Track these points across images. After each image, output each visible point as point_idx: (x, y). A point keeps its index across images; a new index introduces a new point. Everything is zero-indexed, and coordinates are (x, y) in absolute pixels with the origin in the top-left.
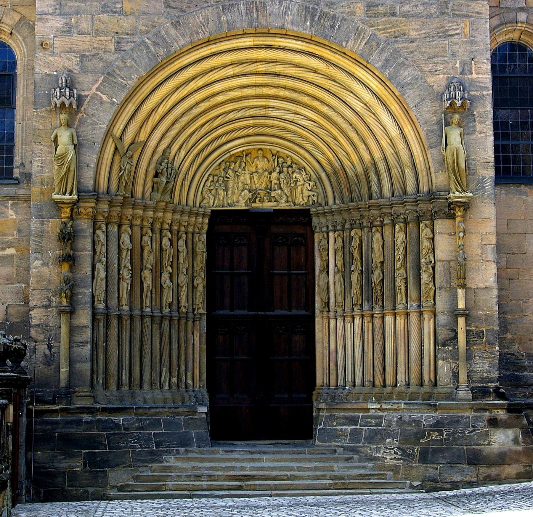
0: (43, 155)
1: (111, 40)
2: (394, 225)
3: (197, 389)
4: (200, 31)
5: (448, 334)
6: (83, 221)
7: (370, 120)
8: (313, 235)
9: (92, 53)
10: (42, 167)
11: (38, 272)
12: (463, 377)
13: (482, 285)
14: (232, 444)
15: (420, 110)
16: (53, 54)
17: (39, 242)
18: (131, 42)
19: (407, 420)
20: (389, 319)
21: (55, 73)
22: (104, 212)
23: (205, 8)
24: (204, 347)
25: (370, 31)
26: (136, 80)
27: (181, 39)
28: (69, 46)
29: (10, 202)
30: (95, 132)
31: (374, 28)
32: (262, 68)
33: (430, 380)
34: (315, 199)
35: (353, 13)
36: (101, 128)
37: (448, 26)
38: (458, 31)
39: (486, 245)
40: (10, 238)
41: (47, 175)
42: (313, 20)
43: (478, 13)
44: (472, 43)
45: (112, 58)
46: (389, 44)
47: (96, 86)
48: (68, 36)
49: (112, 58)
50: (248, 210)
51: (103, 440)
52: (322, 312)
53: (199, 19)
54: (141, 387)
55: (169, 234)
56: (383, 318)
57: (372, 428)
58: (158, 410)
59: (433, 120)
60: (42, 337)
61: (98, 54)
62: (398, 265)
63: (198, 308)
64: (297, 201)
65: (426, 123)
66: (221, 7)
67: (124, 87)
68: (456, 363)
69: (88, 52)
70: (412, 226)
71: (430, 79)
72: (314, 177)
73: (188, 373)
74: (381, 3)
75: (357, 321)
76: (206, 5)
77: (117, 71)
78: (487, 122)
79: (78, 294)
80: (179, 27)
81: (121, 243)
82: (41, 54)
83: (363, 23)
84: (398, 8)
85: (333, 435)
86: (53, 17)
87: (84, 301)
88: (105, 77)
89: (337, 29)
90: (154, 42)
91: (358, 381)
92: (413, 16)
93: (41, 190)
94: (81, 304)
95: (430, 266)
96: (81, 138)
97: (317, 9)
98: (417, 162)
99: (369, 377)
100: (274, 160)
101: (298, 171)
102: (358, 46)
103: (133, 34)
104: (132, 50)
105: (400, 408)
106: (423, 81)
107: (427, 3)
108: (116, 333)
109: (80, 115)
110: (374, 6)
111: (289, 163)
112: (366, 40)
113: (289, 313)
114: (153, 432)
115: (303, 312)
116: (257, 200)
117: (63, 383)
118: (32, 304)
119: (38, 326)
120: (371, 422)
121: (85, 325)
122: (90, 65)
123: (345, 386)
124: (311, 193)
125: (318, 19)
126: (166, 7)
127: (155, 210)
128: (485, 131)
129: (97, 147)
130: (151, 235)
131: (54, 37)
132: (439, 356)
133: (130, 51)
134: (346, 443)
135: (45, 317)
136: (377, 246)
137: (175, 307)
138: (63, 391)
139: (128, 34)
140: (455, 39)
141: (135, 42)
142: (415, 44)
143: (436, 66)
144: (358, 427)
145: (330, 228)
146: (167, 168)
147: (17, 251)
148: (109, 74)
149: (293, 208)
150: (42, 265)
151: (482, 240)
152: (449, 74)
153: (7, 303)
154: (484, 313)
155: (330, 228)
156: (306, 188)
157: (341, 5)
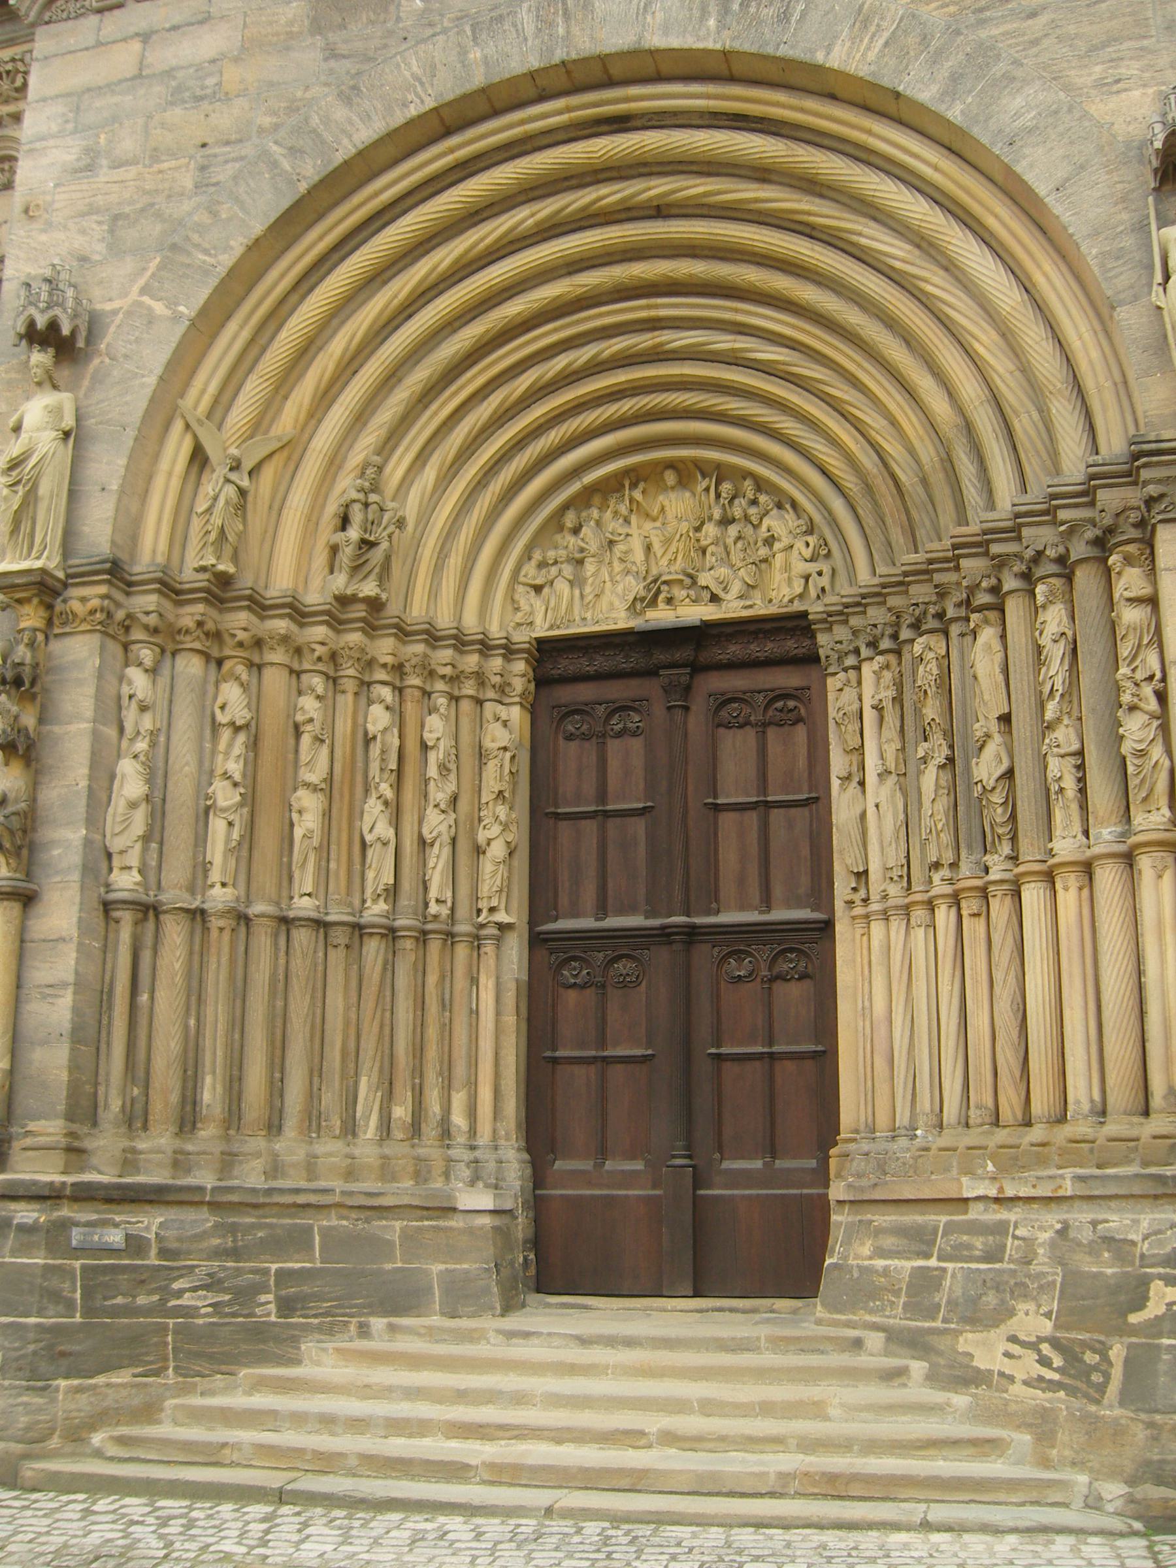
1: (189, 163)
4: (410, 97)
6: (80, 638)
7: (936, 283)
9: (138, 206)
14: (586, 1307)
16: (49, 226)
18: (235, 160)
19: (1086, 1235)
20: (1033, 895)
22: (147, 613)
23: (424, 41)
24: (510, 1020)
27: (361, 126)
28: (87, 200)
32: (610, 194)
34: (825, 581)
36: (143, 386)
45: (187, 206)
46: (958, 33)
47: (141, 282)
48: (87, 177)
52: (850, 903)
54: (274, 1126)
55: (386, 693)
57: (974, 1266)
58: (301, 1199)
61: (153, 205)
63: (492, 910)
65: (1095, 233)
67: (206, 272)
70: (1086, 578)
71: (1099, 108)
73: (453, 1093)
76: (429, 32)
77: (196, 237)
80: (356, 100)
81: (218, 711)
82: (22, 233)
89: (798, 22)
90: (291, 148)
94: (57, 873)
95: (1148, 690)
96: (93, 421)
98: (1083, 367)
99: (982, 1095)
100: (707, 489)
101: (775, 511)
103: (241, 141)
104: (235, 178)
105: (1061, 1193)
106: (1077, 114)
108: (177, 966)
109: (96, 362)
111: (750, 495)
112: (886, 35)
114: (274, 1267)
116: (661, 597)
120: (969, 1247)
121: (64, 934)
124: (812, 568)
126: (326, 59)
127: (336, 623)
131: (57, 186)
134: (896, 1318)
139: (228, 143)
141: (242, 158)
142: (1043, 19)
143: (1115, 68)
144: (933, 1262)
145: (865, 652)
146: (366, 505)
148: (174, 247)
149: (762, 612)
155: (865, 652)
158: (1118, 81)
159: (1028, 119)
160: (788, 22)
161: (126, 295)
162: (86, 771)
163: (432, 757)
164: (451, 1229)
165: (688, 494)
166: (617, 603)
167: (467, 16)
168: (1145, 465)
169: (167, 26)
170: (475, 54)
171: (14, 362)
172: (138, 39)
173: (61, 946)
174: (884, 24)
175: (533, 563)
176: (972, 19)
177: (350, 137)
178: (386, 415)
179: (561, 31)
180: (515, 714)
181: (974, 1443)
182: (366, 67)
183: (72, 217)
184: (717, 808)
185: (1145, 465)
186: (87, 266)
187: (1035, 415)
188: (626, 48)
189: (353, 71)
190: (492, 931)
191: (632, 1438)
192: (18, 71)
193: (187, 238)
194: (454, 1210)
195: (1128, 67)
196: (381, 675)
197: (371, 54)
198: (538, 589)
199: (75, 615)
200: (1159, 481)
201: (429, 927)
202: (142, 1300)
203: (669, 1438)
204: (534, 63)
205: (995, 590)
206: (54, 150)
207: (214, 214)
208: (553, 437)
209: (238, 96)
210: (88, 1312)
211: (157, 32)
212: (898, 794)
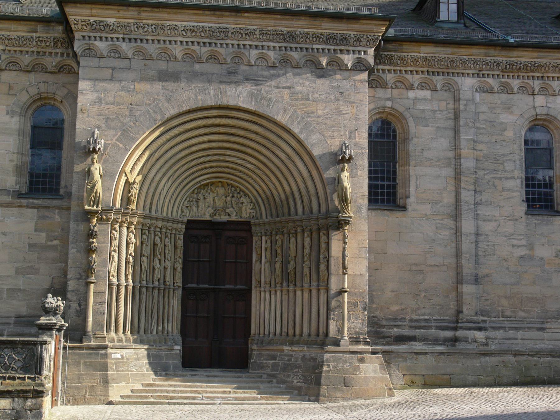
2: (304, 234)
3: (175, 334)
7: (291, 166)
8: (252, 238)
10: (79, 189)
11: (74, 256)
16: (88, 117)
18: (139, 110)
20: (299, 293)
21: (89, 129)
29: (57, 211)
30: (114, 167)
33: (323, 332)
34: (254, 214)
37: (342, 108)
38: (348, 112)
40: (56, 233)
42: (256, 101)
43: (361, 101)
47: (116, 138)
50: (210, 221)
55: (160, 234)
56: (295, 292)
60: (75, 298)
62: (306, 259)
64: (242, 216)
72: (254, 200)
75: (279, 293)
76: (188, 88)
77: (130, 129)
82: (81, 116)
85: (261, 366)
86: (90, 93)
89: (272, 107)
95: (325, 260)
98: (319, 193)
99: (285, 329)
102: (284, 119)
104: (140, 115)
111: (238, 191)
112: (289, 115)
113: (235, 287)
115: (244, 287)
116: (217, 214)
118: (69, 276)
119: (73, 291)
120: (285, 358)
123: (270, 335)
124: (252, 211)
128: (363, 175)
130: (148, 234)
135: (78, 286)
136: (292, 246)
137: (162, 281)
139: (137, 105)
141: (141, 111)
142: (321, 118)
144: (277, 361)
147: (60, 242)
148: (124, 130)
149: (240, 220)
150: (78, 251)
153: (53, 276)
155: (263, 233)
156: (248, 208)
159: (315, 141)
161: (112, 140)
163: (167, 248)
164: (173, 354)
165: (223, 188)
166: (207, 213)
170: (200, 98)
171: (81, 151)
172: (110, 69)
175: (187, 201)
177: (169, 111)
178: (164, 170)
180: (182, 237)
184: (226, 262)
187: (308, 197)
190: (177, 287)
192: (48, 41)
194: (173, 349)
196: (158, 230)
198: (187, 207)
199: (103, 219)
201: (166, 287)
205: (296, 231)
207: (135, 124)
208: (197, 174)
210: (117, 371)
211: (116, 68)
212: (270, 267)
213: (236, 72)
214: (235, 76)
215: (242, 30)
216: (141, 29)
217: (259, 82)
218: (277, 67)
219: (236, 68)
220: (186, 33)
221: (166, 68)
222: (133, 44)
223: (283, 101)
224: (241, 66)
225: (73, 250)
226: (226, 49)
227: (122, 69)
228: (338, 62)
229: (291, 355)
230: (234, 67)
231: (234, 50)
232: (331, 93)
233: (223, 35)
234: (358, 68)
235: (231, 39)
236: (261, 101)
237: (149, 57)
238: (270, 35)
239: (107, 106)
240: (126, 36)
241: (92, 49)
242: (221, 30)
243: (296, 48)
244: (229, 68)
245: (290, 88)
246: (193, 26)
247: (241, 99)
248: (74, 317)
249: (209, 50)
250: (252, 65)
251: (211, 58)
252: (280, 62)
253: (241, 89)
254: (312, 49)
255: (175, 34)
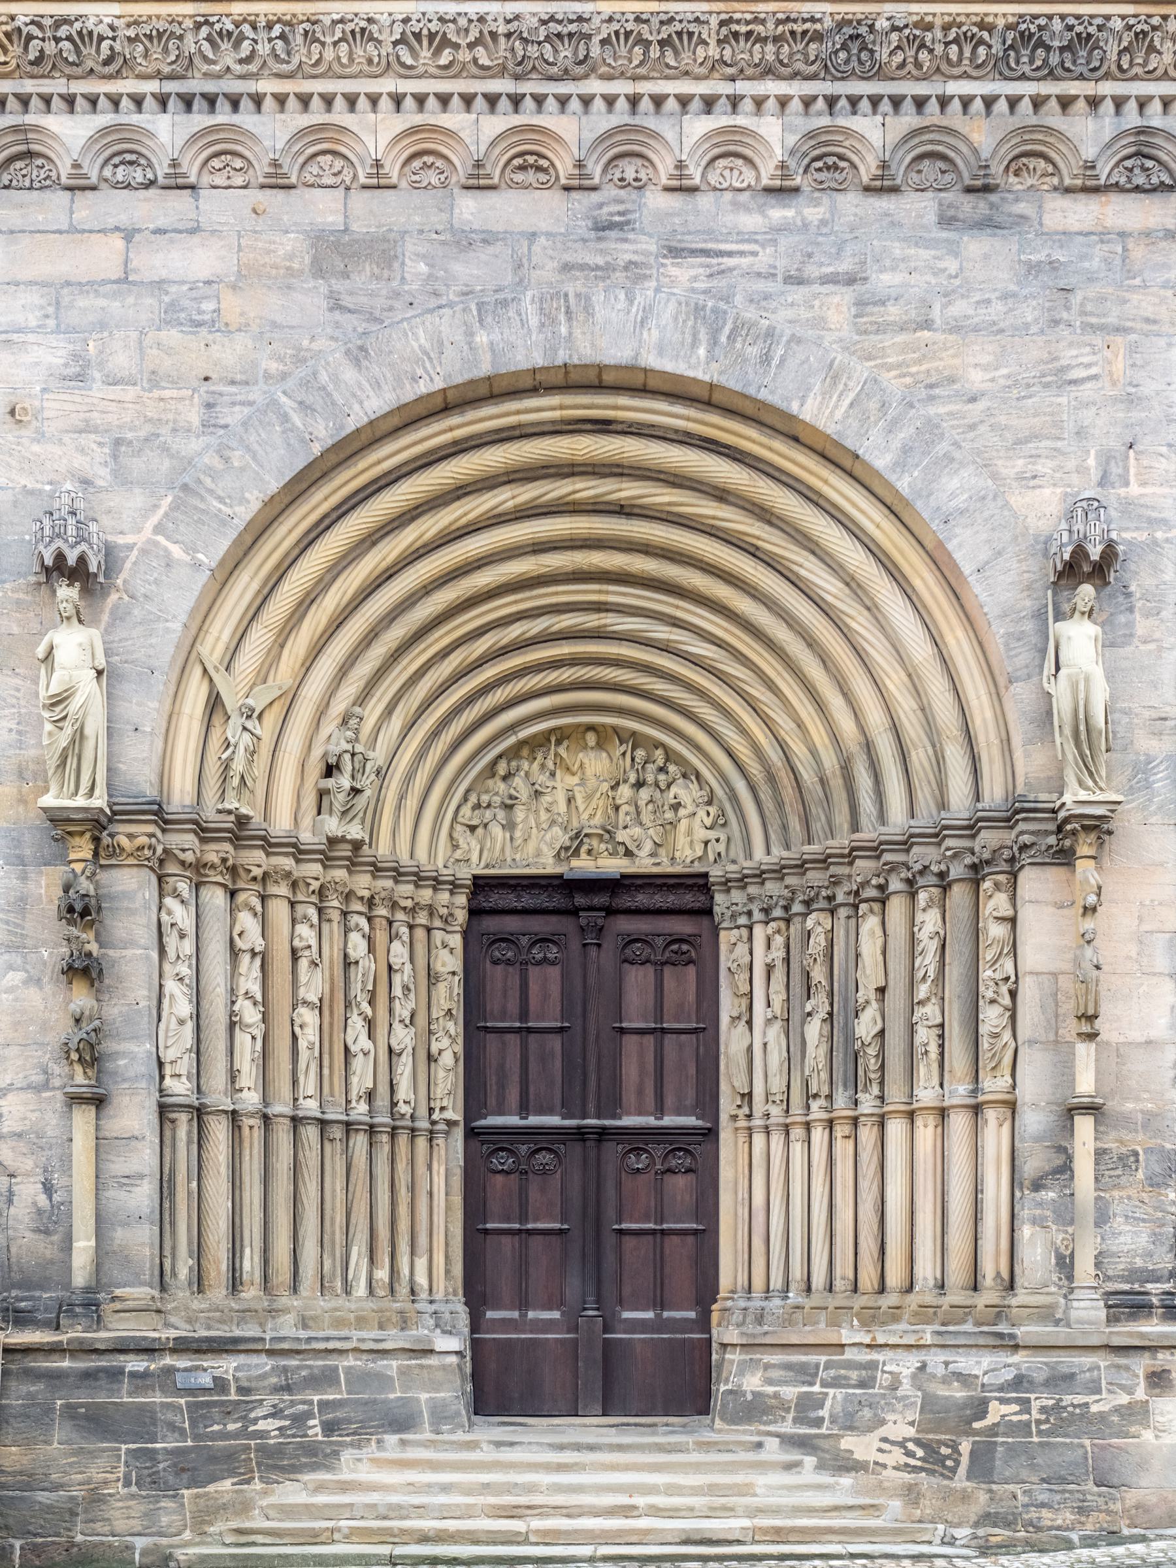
0: (23, 703)
4: (420, 372)
5: (1049, 1160)
6: (127, 870)
9: (142, 434)
10: (19, 733)
11: (16, 1000)
12: (1085, 1267)
13: (1137, 1036)
15: (990, 581)
16: (40, 437)
17: (17, 925)
18: (242, 403)
19: (940, 1371)
21: (48, 488)
23: (431, 311)
25: (862, 370)
26: (256, 506)
27: (371, 394)
28: (82, 415)
30: (153, 641)
31: (872, 363)
35: (820, 323)
36: (167, 630)
37: (1068, 355)
38: (1094, 371)
39: (1152, 932)
41: (32, 753)
42: (714, 342)
43: (1147, 320)
44: (1130, 401)
45: (194, 445)
46: (911, 406)
47: (154, 519)
49: (194, 445)
51: (178, 1418)
53: (417, 340)
59: (1024, 609)
60: (28, 1164)
61: (158, 435)
66: (473, 307)
67: (224, 521)
68: (1066, 1232)
69: (130, 430)
71: (1018, 499)
74: (894, 295)
76: (433, 302)
77: (208, 481)
78: (1164, 614)
79: (116, 1055)
80: (365, 363)
82: (10, 437)
83: (845, 349)
84: (937, 308)
86: (39, 338)
87: (131, 1074)
88: (176, 497)
89: (778, 366)
90: (301, 403)
91: (819, 1280)
92: (976, 329)
93: (20, 792)
94: (124, 1080)
97: (725, 312)
103: (247, 383)
104: (245, 424)
106: (1000, 503)
107: (1014, 295)
109: (113, 597)
110: (875, 304)
112: (851, 396)
117: (80, 1278)
119: (19, 1135)
121: (136, 1133)
122: (137, 465)
125: (729, 337)
126: (331, 310)
128: (1157, 635)
129: (161, 683)
131: (44, 390)
132: (1024, 1213)
133: (240, 429)
135: (37, 1114)
138: (77, 1299)
139: (233, 383)
140: (1087, 391)
141: (251, 404)
142: (981, 405)
143: (1034, 464)
148: (185, 487)
150: (26, 982)
151: (1141, 919)
152: (1069, 486)
154: (1140, 1106)
157: (790, 300)
158: (1035, 477)
159: (961, 501)
160: (769, 365)
161: (139, 531)
162: (145, 993)
167: (471, 292)
168: (1024, 819)
169: (151, 226)
170: (482, 338)
173: (134, 1143)
174: (851, 384)
176: (924, 393)
177: (361, 403)
179: (564, 330)
181: (862, 1507)
182: (375, 327)
183: (67, 431)
185: (1024, 819)
186: (92, 490)
188: (624, 363)
189: (360, 330)
191: (627, 1511)
193: (199, 481)
195: (1044, 465)
197: (377, 313)
200: (1032, 833)
202: (231, 1427)
203: (655, 1511)
204: (540, 362)
206: (35, 347)
207: (227, 460)
209: (239, 330)
211: (139, 231)
213: (628, 223)
214: (626, 240)
215: (647, 21)
216: (225, 45)
217: (725, 260)
218: (796, 190)
219: (629, 206)
220: (414, 54)
221: (340, 219)
222: (200, 120)
223: (820, 337)
224: (648, 193)
225: (11, 974)
226: (584, 119)
227: (165, 232)
228: (1053, 155)
229: (872, 1366)
230: (622, 202)
231: (615, 120)
232: (1025, 292)
233: (566, 52)
234: (1140, 180)
235: (603, 69)
236: (731, 338)
237: (268, 175)
238: (764, 40)
239: (116, 392)
240: (171, 87)
241: (39, 155)
242: (559, 28)
243: (875, 101)
244: (601, 206)
245: (851, 280)
246: (441, 19)
247: (652, 336)
248: (28, 1234)
249: (515, 130)
250: (694, 190)
251: (522, 168)
252: (805, 171)
253: (650, 293)
254: (944, 102)
255: (370, 61)
